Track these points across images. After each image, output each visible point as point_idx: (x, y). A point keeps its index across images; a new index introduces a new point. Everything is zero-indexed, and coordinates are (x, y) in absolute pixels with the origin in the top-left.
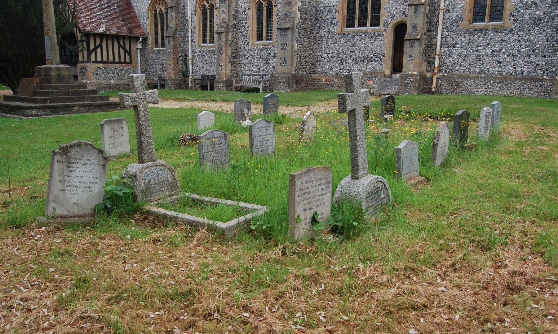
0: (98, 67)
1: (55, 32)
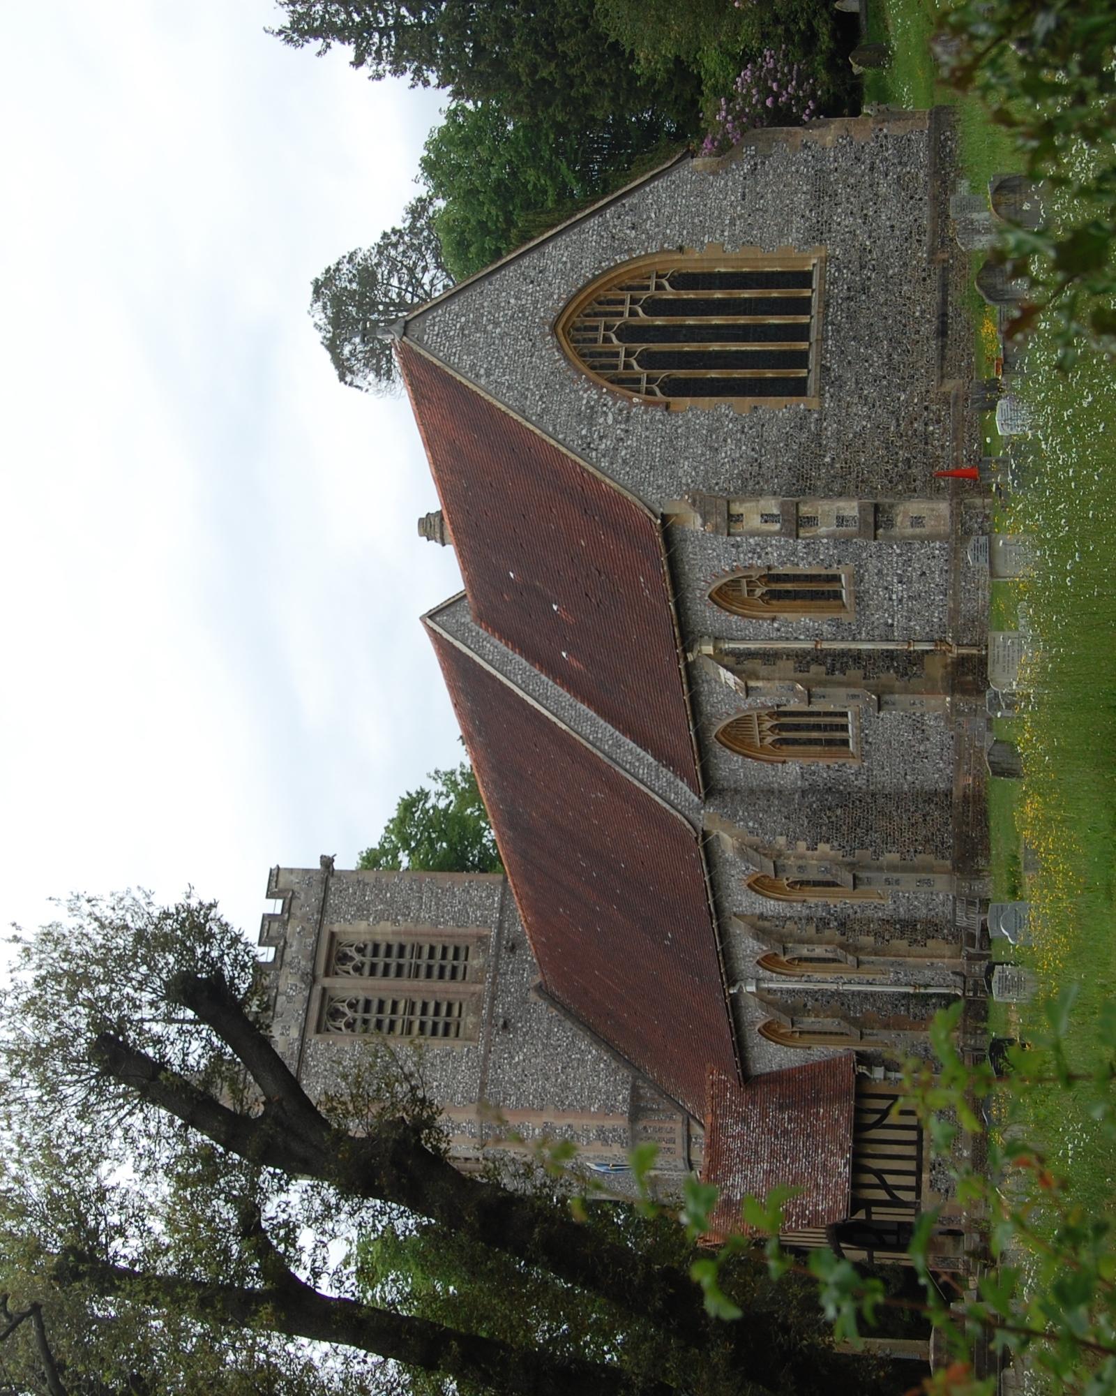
0: (931, 1186)
1: (872, 1340)
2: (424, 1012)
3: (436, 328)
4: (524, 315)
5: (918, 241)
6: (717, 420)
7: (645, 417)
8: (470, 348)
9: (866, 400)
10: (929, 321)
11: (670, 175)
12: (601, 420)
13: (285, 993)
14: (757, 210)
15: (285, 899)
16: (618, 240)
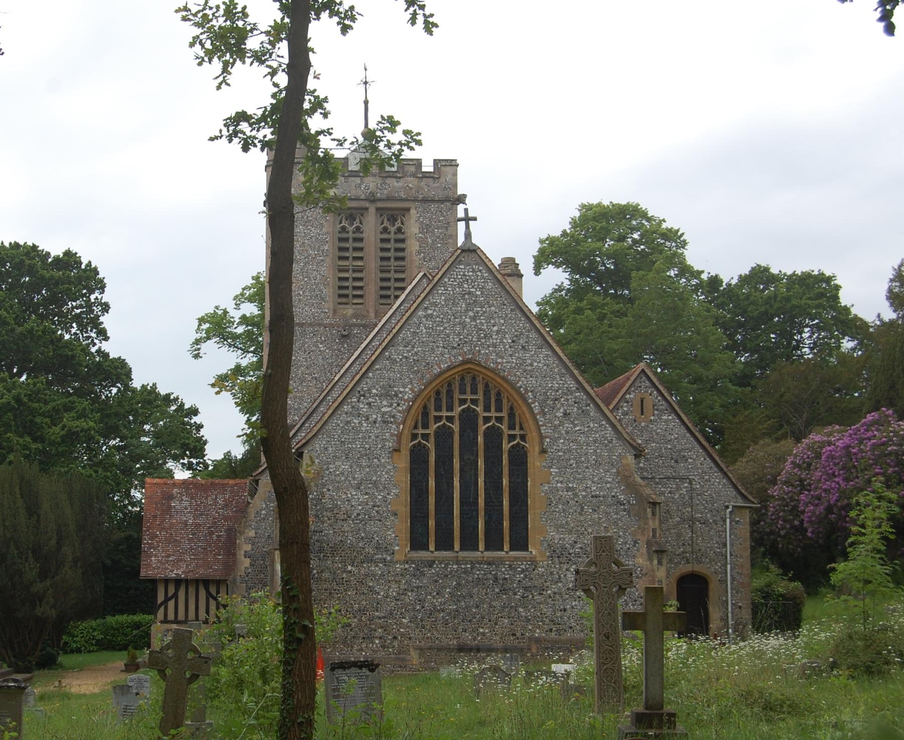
2: (355, 279)
3: (470, 274)
4: (482, 338)
5: (551, 630)
6: (385, 488)
8: (452, 301)
9: (403, 594)
10: (475, 639)
11: (617, 439)
12: (385, 403)
14: (582, 508)
15: (434, 173)
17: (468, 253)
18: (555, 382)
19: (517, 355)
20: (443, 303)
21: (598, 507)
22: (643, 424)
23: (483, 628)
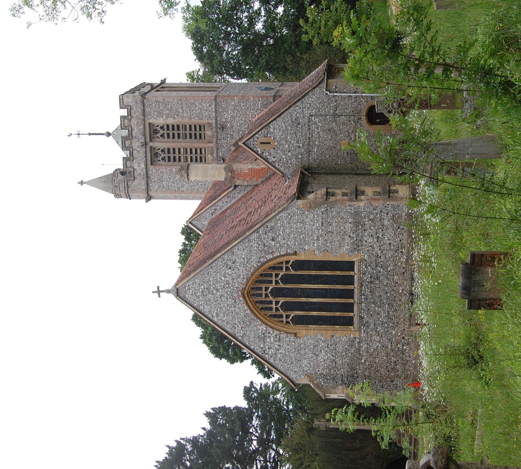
2: (191, 153)
3: (191, 291)
4: (229, 286)
6: (317, 341)
7: (286, 339)
9: (378, 333)
10: (405, 295)
12: (268, 340)
13: (136, 150)
14: (330, 232)
16: (267, 246)
17: (179, 292)
18: (254, 245)
19: (238, 267)
20: (209, 307)
21: (329, 222)
22: (276, 144)
23: (399, 290)
